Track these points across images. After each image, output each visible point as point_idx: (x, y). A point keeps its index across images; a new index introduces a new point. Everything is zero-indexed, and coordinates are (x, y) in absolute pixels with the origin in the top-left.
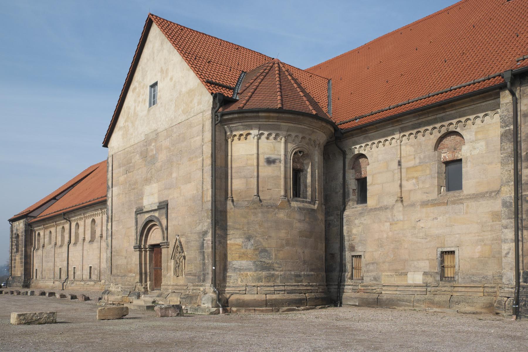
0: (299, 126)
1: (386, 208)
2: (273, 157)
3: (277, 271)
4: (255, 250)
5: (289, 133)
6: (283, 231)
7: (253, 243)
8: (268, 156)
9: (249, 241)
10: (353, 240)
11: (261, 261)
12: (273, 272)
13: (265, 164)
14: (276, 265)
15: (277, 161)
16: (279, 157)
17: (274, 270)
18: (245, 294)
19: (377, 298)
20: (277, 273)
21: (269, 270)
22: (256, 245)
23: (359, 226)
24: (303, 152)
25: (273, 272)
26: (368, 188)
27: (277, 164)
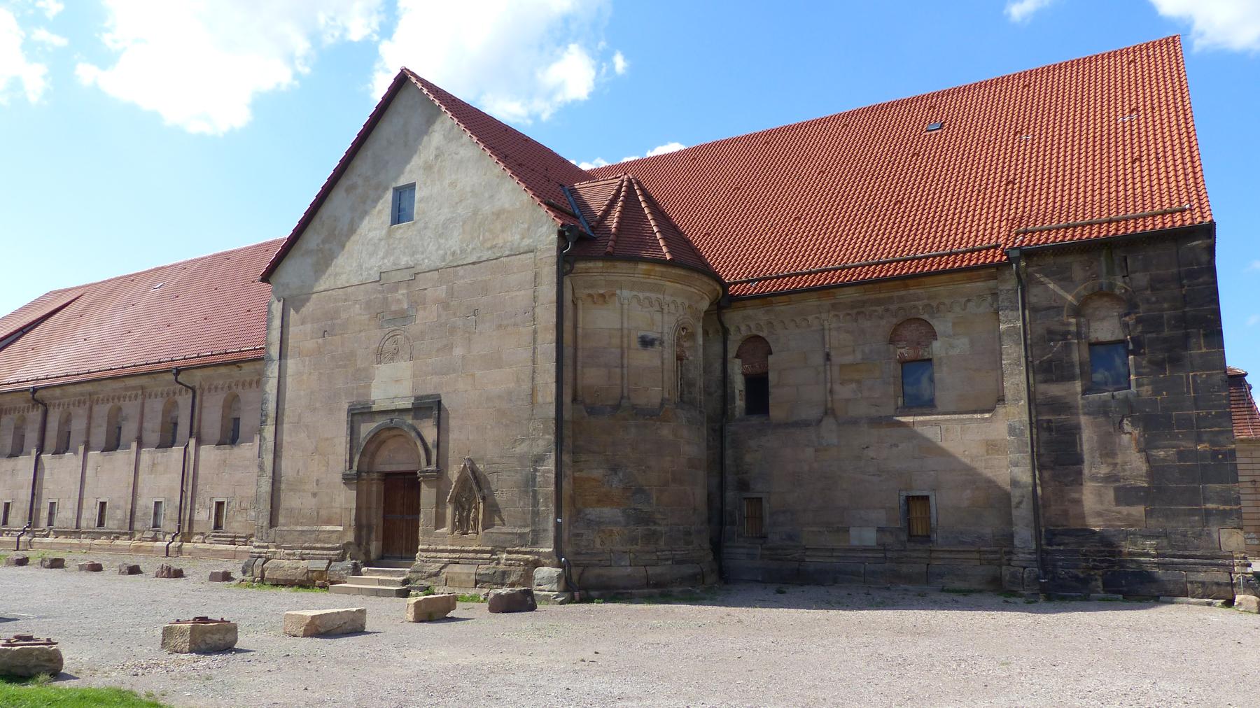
0: (689, 288)
1: (805, 424)
2: (651, 335)
3: (660, 525)
4: (626, 489)
5: (673, 298)
6: (669, 458)
7: (621, 477)
8: (643, 333)
9: (616, 473)
10: (746, 473)
11: (635, 509)
12: (653, 528)
13: (639, 346)
14: (659, 516)
15: (657, 343)
16: (659, 336)
17: (655, 523)
18: (611, 566)
19: (798, 570)
20: (659, 528)
21: (648, 525)
22: (626, 481)
23: (756, 451)
24: (687, 329)
25: (653, 528)
26: (771, 390)
27: (658, 348)
